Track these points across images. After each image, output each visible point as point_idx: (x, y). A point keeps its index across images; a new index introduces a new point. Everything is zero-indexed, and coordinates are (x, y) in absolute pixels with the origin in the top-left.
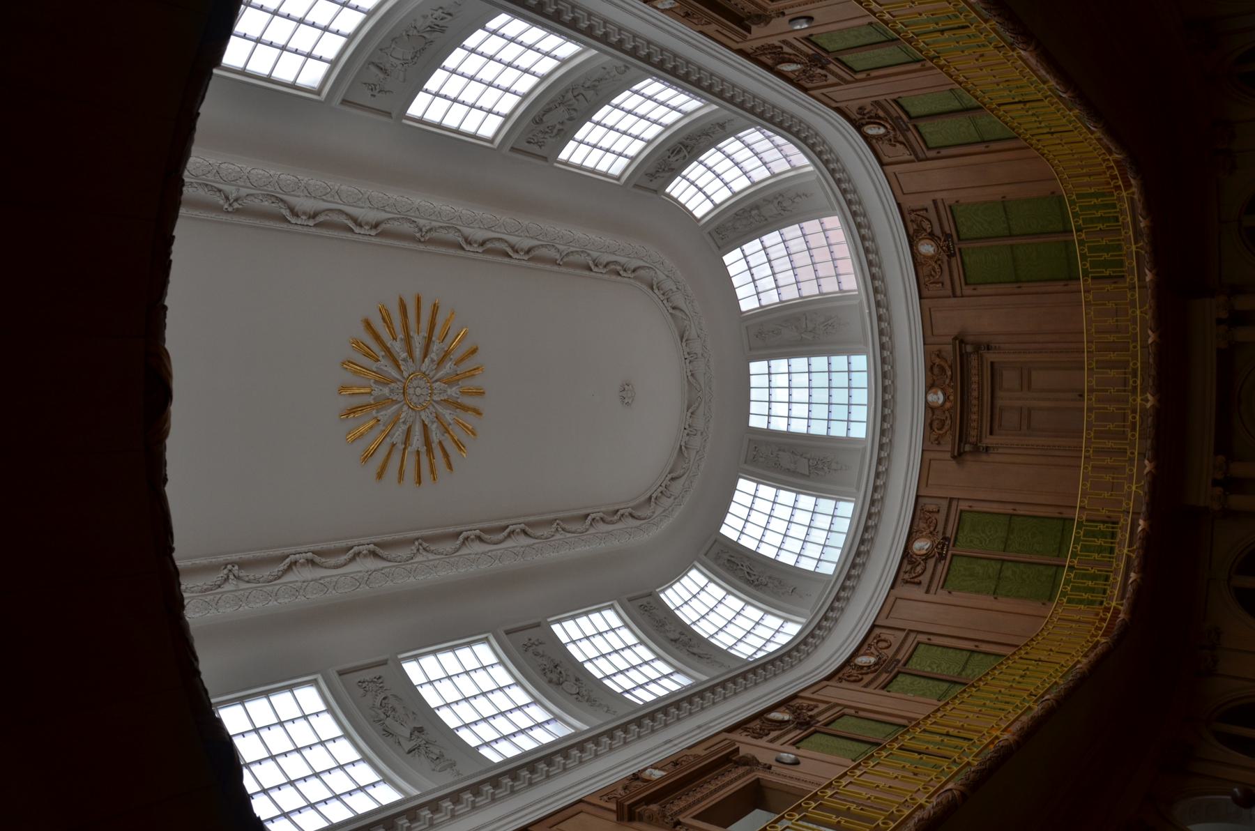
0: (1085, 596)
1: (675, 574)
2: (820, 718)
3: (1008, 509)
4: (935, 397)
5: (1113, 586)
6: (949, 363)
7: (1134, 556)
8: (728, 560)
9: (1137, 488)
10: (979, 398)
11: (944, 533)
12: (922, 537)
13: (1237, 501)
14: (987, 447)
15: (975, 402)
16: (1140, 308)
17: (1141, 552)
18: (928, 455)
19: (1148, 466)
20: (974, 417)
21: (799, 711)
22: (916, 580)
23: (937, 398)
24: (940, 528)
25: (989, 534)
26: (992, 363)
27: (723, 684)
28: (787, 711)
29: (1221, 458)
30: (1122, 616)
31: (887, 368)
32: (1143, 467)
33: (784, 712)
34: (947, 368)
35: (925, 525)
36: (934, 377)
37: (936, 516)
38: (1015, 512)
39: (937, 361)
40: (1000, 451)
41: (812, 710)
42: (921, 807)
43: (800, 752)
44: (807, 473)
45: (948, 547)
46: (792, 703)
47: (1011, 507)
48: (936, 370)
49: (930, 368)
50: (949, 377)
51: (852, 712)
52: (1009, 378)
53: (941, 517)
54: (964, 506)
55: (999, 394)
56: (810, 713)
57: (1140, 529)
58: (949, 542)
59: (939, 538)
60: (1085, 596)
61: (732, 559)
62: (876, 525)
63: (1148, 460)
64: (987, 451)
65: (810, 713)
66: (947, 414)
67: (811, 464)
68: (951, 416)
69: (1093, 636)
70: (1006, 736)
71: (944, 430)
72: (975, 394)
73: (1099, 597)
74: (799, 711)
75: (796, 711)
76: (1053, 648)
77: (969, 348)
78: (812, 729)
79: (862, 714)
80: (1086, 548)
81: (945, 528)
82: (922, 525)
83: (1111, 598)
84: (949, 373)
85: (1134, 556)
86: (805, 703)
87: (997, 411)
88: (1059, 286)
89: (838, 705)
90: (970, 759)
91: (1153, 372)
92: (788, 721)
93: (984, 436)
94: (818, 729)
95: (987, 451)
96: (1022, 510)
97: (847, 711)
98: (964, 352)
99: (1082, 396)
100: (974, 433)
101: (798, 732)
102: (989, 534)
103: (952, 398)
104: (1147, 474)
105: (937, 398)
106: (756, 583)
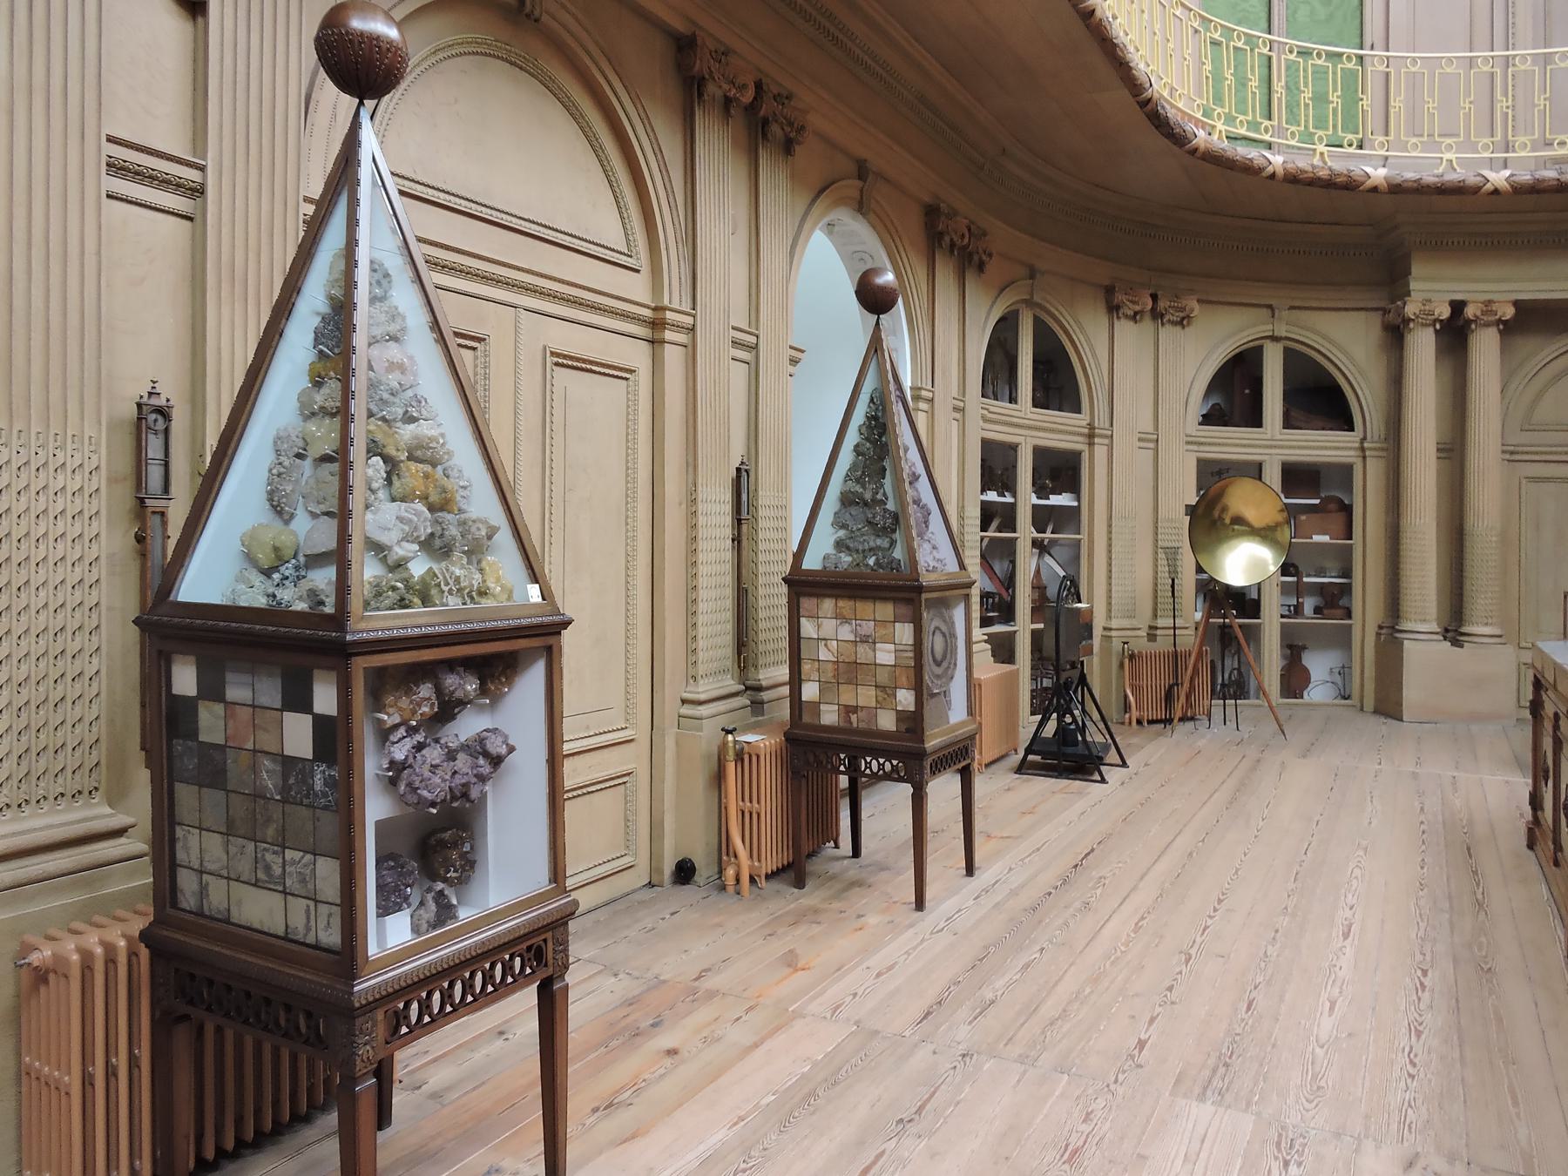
13: (1422, 347)
29: (1509, 312)
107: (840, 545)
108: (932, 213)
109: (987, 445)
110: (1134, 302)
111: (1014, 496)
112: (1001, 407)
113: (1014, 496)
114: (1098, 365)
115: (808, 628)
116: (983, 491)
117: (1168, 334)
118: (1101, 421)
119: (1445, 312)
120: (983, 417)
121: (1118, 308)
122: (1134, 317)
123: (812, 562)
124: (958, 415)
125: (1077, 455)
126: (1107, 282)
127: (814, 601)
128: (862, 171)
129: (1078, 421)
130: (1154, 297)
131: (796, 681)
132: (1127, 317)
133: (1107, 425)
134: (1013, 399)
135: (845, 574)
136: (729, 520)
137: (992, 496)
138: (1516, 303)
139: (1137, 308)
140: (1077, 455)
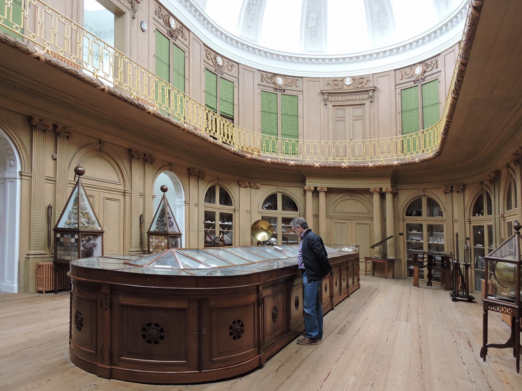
4: (349, 81)
5: (269, 154)
6: (364, 86)
7: (279, 160)
9: (308, 161)
10: (349, 99)
14: (327, 105)
15: (347, 98)
16: (383, 160)
17: (280, 162)
18: (322, 80)
19: (317, 165)
20: (340, 98)
22: (263, 80)
23: (348, 82)
26: (365, 104)
31: (361, 58)
32: (317, 162)
34: (361, 85)
36: (359, 80)
38: (299, 117)
39: (365, 80)
40: (326, 110)
48: (361, 80)
49: (362, 78)
50: (358, 86)
52: (358, 111)
55: (351, 107)
57: (290, 162)
59: (283, 88)
63: (320, 164)
64: (325, 104)
66: (341, 87)
68: (340, 88)
71: (333, 86)
72: (350, 98)
77: (371, 94)
80: (287, 144)
84: (360, 86)
85: (279, 160)
87: (344, 107)
88: (399, 129)
91: (356, 165)
93: (332, 103)
95: (325, 104)
98: (369, 91)
99: (351, 140)
100: (333, 98)
103: (348, 88)
104: (314, 164)
105: (348, 82)
106: (249, 8)
108: (189, 169)
114: (237, 199)
119: (313, 189)
128: (170, 164)
138: (327, 188)
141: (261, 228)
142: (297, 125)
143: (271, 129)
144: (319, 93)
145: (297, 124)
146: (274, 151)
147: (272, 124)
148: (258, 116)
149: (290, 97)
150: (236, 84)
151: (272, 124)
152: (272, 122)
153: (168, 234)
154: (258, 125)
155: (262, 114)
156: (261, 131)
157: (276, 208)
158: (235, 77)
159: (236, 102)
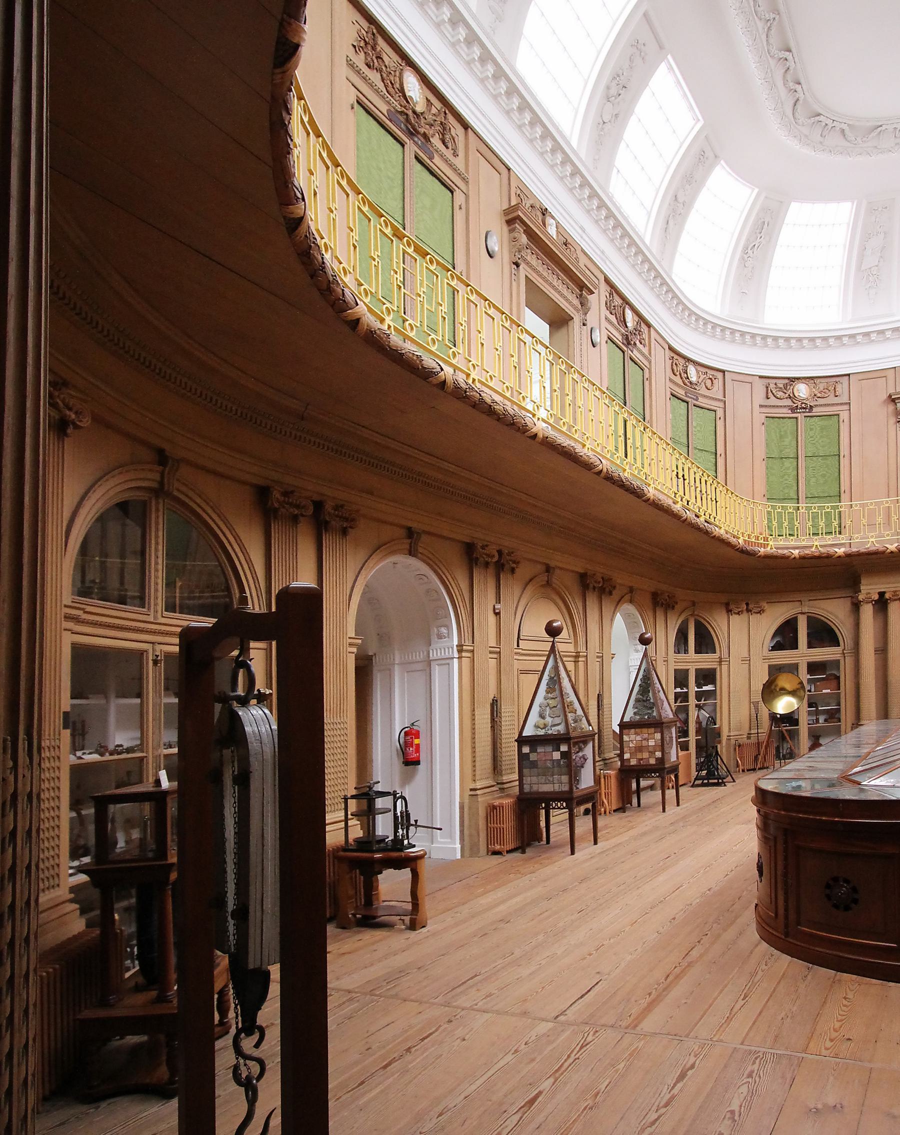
0: (775, 523)
1: (743, 173)
2: (635, 352)
3: (844, 451)
5: (785, 541)
8: (764, 222)
11: (816, 406)
12: (811, 389)
21: (637, 333)
24: (821, 401)
25: (820, 441)
27: (646, 260)
28: (635, 323)
30: (762, 550)
33: (634, 320)
35: (822, 389)
37: (832, 395)
38: (841, 457)
41: (641, 343)
42: (584, 446)
43: (605, 348)
44: (863, 268)
45: (804, 412)
46: (642, 324)
47: (847, 453)
51: (647, 375)
53: (832, 400)
54: (844, 415)
56: (638, 343)
58: (809, 412)
60: (775, 523)
61: (766, 224)
62: (817, 347)
65: (638, 343)
67: (873, 269)
69: (743, 534)
70: (650, 489)
73: (775, 532)
74: (637, 333)
75: (637, 331)
76: (728, 509)
78: (626, 349)
79: (647, 383)
80: (815, 517)
81: (821, 405)
82: (821, 387)
83: (775, 540)
86: (645, 336)
89: (650, 363)
90: (628, 470)
92: (627, 327)
94: (626, 353)
96: (844, 462)
97: (646, 371)
101: (620, 338)
102: (820, 441)
107: (635, 713)
109: (675, 670)
110: (737, 608)
111: (688, 689)
112: (682, 656)
113: (688, 689)
115: (626, 738)
116: (675, 688)
117: (754, 618)
118: (725, 655)
120: (675, 662)
121: (731, 611)
122: (738, 613)
123: (626, 719)
124: (665, 663)
125: (715, 670)
126: (726, 601)
127: (627, 730)
129: (717, 655)
130: (747, 604)
131: (621, 756)
132: (735, 613)
133: (727, 657)
134: (686, 651)
135: (638, 721)
136: (596, 706)
137: (678, 690)
139: (740, 610)
140: (715, 670)
141: (783, 689)
142: (837, 474)
143: (786, 491)
144: (885, 401)
145: (837, 471)
146: (791, 533)
147: (786, 480)
148: (760, 468)
149: (822, 420)
150: (720, 413)
151: (786, 480)
152: (786, 477)
153: (663, 723)
154: (761, 487)
155: (768, 463)
156: (765, 498)
157: (794, 645)
158: (719, 400)
159: (720, 450)
